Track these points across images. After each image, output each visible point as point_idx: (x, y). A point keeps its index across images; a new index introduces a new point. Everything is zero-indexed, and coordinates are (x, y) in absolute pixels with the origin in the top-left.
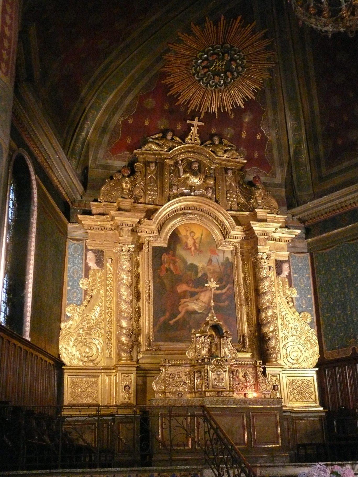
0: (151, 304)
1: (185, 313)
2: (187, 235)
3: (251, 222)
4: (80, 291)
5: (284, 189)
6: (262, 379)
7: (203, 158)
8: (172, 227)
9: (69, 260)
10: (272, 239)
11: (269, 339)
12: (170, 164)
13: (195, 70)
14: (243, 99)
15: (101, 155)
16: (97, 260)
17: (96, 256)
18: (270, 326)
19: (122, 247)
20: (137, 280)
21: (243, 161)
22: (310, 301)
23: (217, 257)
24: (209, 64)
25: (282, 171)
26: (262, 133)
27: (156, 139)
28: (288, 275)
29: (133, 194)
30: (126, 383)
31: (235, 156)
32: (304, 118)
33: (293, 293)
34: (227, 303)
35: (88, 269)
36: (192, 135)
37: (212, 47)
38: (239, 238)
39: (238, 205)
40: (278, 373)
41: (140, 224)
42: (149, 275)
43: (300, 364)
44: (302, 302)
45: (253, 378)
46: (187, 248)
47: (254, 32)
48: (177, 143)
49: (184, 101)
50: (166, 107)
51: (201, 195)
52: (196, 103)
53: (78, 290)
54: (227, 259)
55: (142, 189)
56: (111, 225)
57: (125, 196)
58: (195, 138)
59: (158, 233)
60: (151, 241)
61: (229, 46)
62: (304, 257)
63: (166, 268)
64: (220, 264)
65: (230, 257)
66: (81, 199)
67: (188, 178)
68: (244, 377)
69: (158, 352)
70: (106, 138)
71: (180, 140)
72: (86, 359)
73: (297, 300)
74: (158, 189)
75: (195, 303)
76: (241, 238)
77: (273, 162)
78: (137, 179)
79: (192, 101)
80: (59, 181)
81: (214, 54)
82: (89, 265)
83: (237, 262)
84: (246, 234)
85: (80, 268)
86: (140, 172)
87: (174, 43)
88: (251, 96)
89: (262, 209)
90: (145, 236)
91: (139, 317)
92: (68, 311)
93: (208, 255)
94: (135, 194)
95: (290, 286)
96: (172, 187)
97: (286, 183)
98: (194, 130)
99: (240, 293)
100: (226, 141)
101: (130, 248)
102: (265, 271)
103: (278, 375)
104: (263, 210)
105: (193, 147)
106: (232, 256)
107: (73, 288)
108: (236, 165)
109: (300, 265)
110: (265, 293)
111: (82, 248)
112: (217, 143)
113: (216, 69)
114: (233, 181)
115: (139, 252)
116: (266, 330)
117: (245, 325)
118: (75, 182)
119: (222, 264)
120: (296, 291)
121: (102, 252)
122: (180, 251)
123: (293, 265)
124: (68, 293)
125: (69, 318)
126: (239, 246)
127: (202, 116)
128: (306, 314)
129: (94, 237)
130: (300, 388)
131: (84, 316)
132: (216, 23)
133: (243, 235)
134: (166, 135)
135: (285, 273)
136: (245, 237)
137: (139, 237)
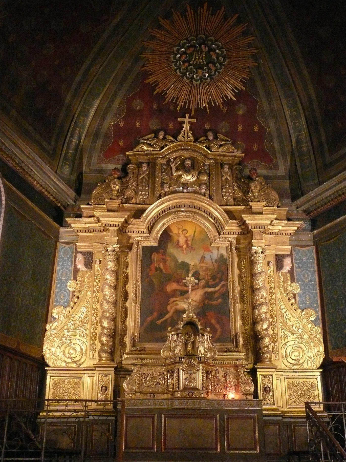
0: (138, 304)
1: (174, 313)
2: (179, 233)
3: (243, 216)
4: (67, 293)
5: (288, 181)
6: (244, 380)
7: (195, 155)
8: (163, 225)
9: (58, 263)
10: (272, 233)
11: (262, 338)
12: (163, 163)
13: (176, 65)
14: (233, 90)
15: (95, 159)
16: (85, 262)
17: (85, 258)
18: (263, 324)
19: (107, 247)
20: (126, 281)
21: (239, 154)
22: (314, 297)
23: (210, 254)
24: (188, 58)
25: (284, 162)
26: (259, 124)
27: (148, 139)
28: (290, 269)
29: (124, 195)
30: (103, 383)
31: (231, 150)
32: (301, 103)
33: (295, 288)
34: (220, 301)
35: (76, 271)
36: (184, 133)
37: (187, 39)
38: (235, 233)
39: (234, 199)
40: (271, 373)
41: (129, 224)
42: (137, 275)
43: (302, 364)
44: (305, 298)
45: (234, 378)
47: (225, 18)
48: (170, 142)
49: (171, 98)
50: (155, 107)
51: (195, 192)
52: (184, 100)
53: (66, 292)
54: (222, 256)
55: (134, 189)
56: (99, 226)
57: (113, 197)
58: (188, 135)
59: (148, 232)
60: (140, 240)
61: (204, 36)
62: (308, 250)
63: (156, 267)
64: (214, 261)
65: (225, 253)
66: (74, 204)
67: (180, 176)
68: (223, 377)
69: (143, 352)
70: (99, 143)
71: (173, 139)
72: (69, 361)
73: (300, 297)
74: (150, 189)
75: (184, 302)
76: (237, 233)
77: (274, 154)
78: (129, 181)
79: (180, 98)
80: (41, 186)
81: (191, 46)
82: (78, 267)
83: (232, 257)
84: (242, 229)
85: (69, 271)
86: (133, 173)
87: (147, 40)
88: (240, 86)
89: (259, 201)
90: (135, 237)
91: (125, 317)
92: (55, 312)
93: (201, 252)
94: (126, 195)
95: (293, 281)
96: (163, 186)
98: (186, 127)
99: (233, 291)
101: (115, 247)
102: (259, 266)
103: (271, 377)
104: (258, 203)
105: (186, 145)
107: (61, 290)
108: (233, 159)
109: (304, 259)
110: (258, 289)
111: (72, 251)
112: (211, 138)
113: (197, 62)
114: (229, 176)
115: (128, 252)
116: (259, 328)
117: (239, 323)
118: (62, 186)
119: (216, 261)
120: (299, 287)
121: (91, 254)
122: (171, 250)
123: (296, 259)
124: (56, 296)
125: (55, 319)
126: (234, 242)
127: (193, 113)
128: (311, 311)
129: (83, 239)
130: (301, 391)
131: (68, 318)
132: (183, 14)
133: (239, 230)
134: (158, 135)
135: (287, 268)
136: (241, 232)
137: (129, 238)
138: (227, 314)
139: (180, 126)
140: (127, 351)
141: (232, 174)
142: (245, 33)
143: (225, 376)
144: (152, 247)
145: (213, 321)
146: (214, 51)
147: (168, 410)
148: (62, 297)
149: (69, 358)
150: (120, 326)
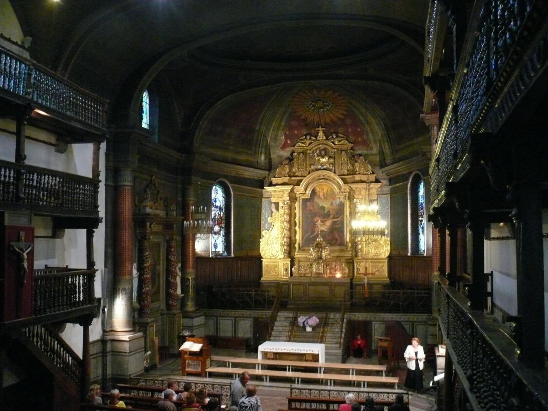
7: (327, 147)
27: (302, 140)
34: (340, 225)
35: (272, 212)
39: (348, 170)
46: (319, 198)
54: (341, 202)
57: (286, 175)
67: (319, 160)
71: (315, 139)
88: (345, 113)
92: (263, 233)
98: (321, 133)
100: (340, 135)
106: (344, 200)
119: (338, 205)
122: (316, 200)
138: (343, 232)
140: (297, 250)
141: (347, 155)
142: (339, 95)
143: (336, 266)
144: (307, 199)
145: (337, 236)
146: (326, 102)
148: (266, 225)
149: (272, 254)
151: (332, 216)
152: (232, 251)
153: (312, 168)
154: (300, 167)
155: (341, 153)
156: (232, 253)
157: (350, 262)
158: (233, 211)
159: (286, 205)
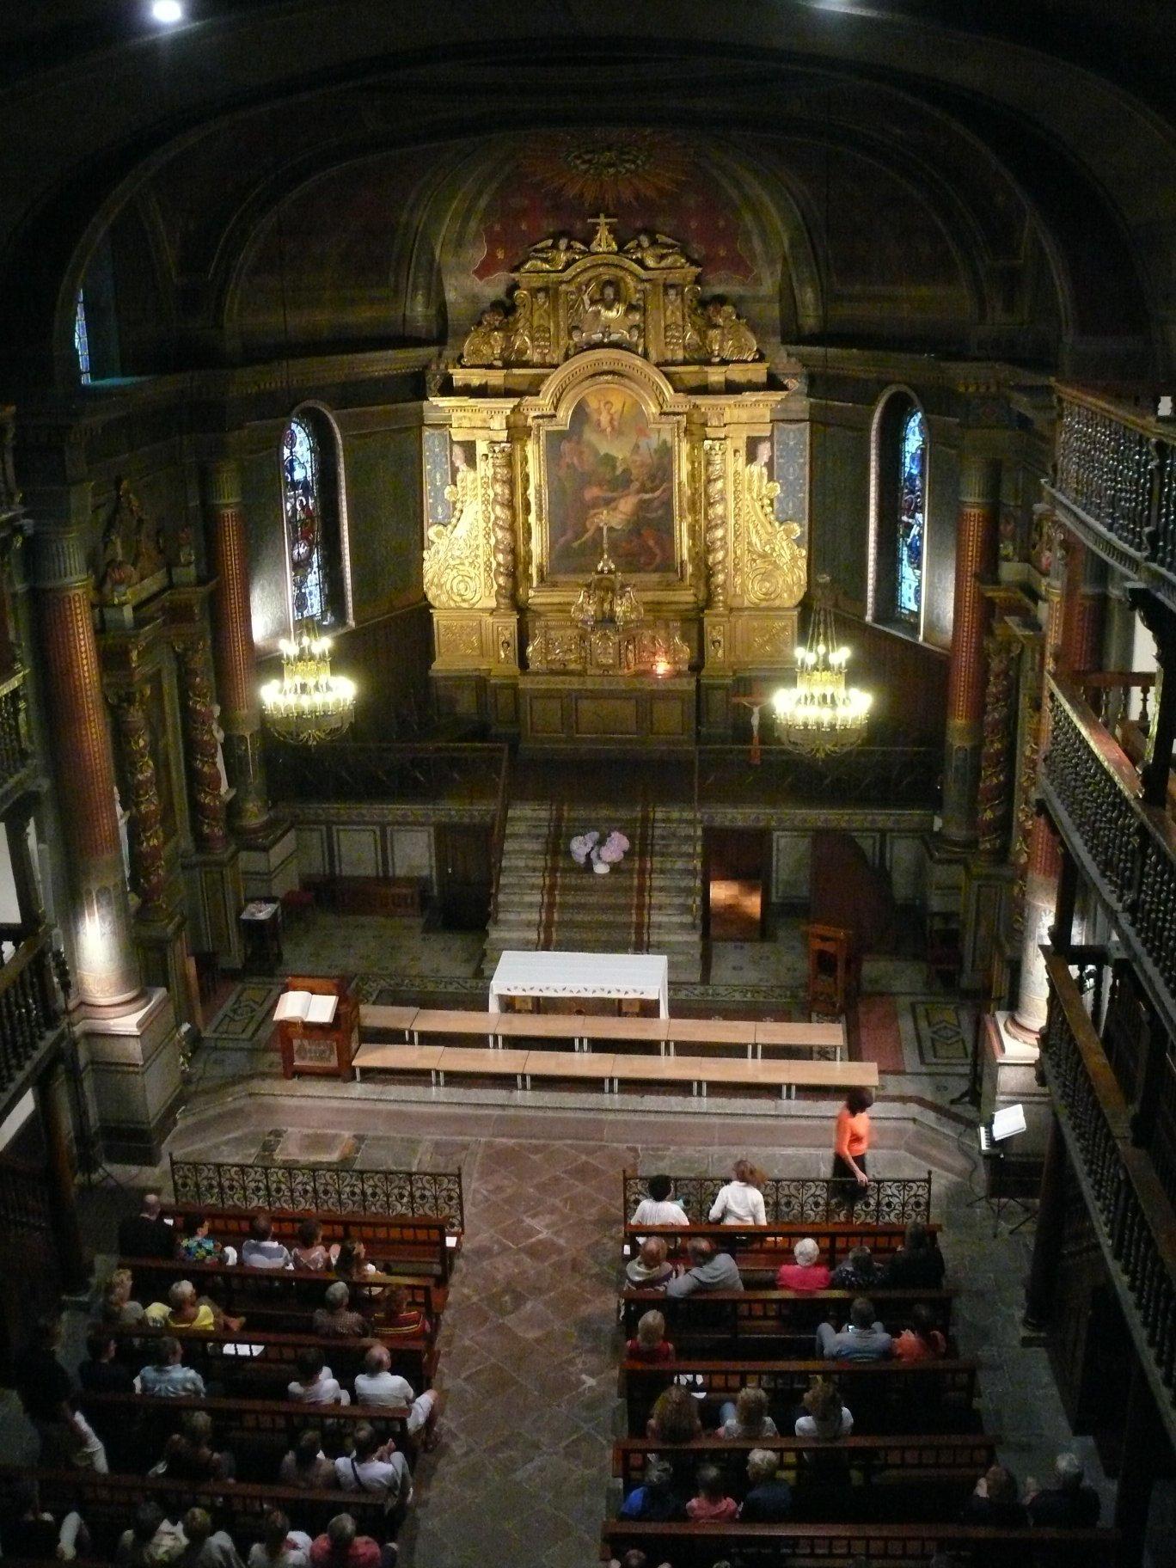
27: (542, 250)
39: (685, 348)
54: (665, 442)
71: (582, 247)
92: (431, 533)
95: (771, 478)
97: (781, 292)
100: (662, 238)
106: (673, 437)
119: (656, 451)
122: (589, 435)
139: (593, 231)
140: (535, 584)
141: (682, 300)
143: (654, 638)
145: (651, 543)
147: (580, 690)
148: (440, 510)
150: (522, 550)
151: (636, 485)
152: (350, 611)
153: (576, 339)
154: (537, 335)
155: (666, 293)
156: (351, 616)
157: (694, 621)
158: (343, 491)
159: (500, 456)
